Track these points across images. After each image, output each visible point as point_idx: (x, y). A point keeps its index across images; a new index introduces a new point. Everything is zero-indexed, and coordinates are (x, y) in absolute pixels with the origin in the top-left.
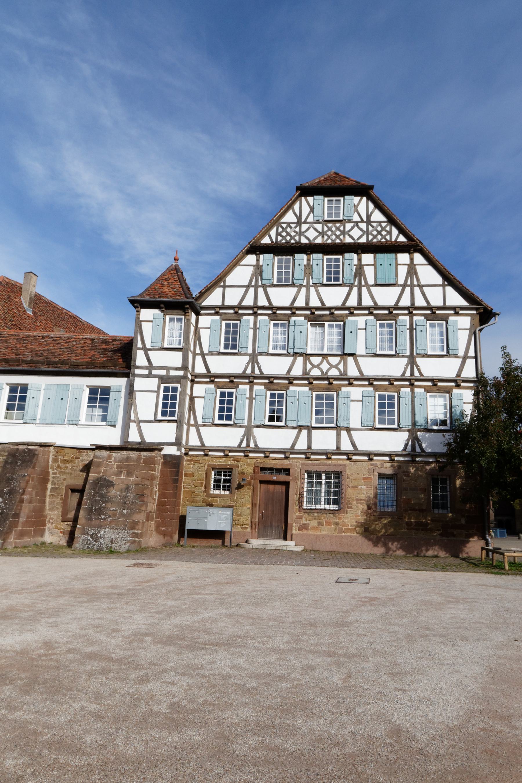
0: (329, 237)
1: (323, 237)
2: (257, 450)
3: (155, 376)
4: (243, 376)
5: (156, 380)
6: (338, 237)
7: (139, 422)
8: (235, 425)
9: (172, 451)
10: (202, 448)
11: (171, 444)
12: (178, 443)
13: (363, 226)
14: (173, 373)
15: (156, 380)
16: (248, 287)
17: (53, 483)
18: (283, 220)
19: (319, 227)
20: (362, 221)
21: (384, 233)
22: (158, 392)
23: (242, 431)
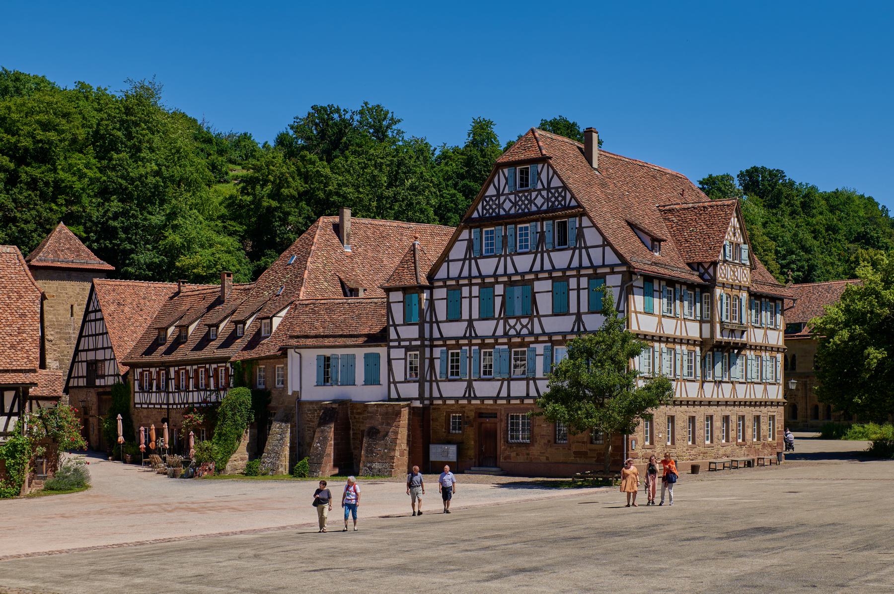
0: (520, 206)
1: (516, 207)
2: (476, 398)
3: (403, 347)
4: (464, 337)
5: (403, 350)
6: (526, 206)
7: (395, 383)
8: (461, 380)
9: (417, 404)
10: (441, 398)
11: (416, 399)
12: (421, 398)
13: (544, 193)
14: (414, 343)
15: (403, 350)
16: (464, 260)
17: (353, 430)
18: (487, 194)
19: (512, 197)
20: (544, 189)
21: (560, 199)
22: (405, 359)
23: (465, 383)
